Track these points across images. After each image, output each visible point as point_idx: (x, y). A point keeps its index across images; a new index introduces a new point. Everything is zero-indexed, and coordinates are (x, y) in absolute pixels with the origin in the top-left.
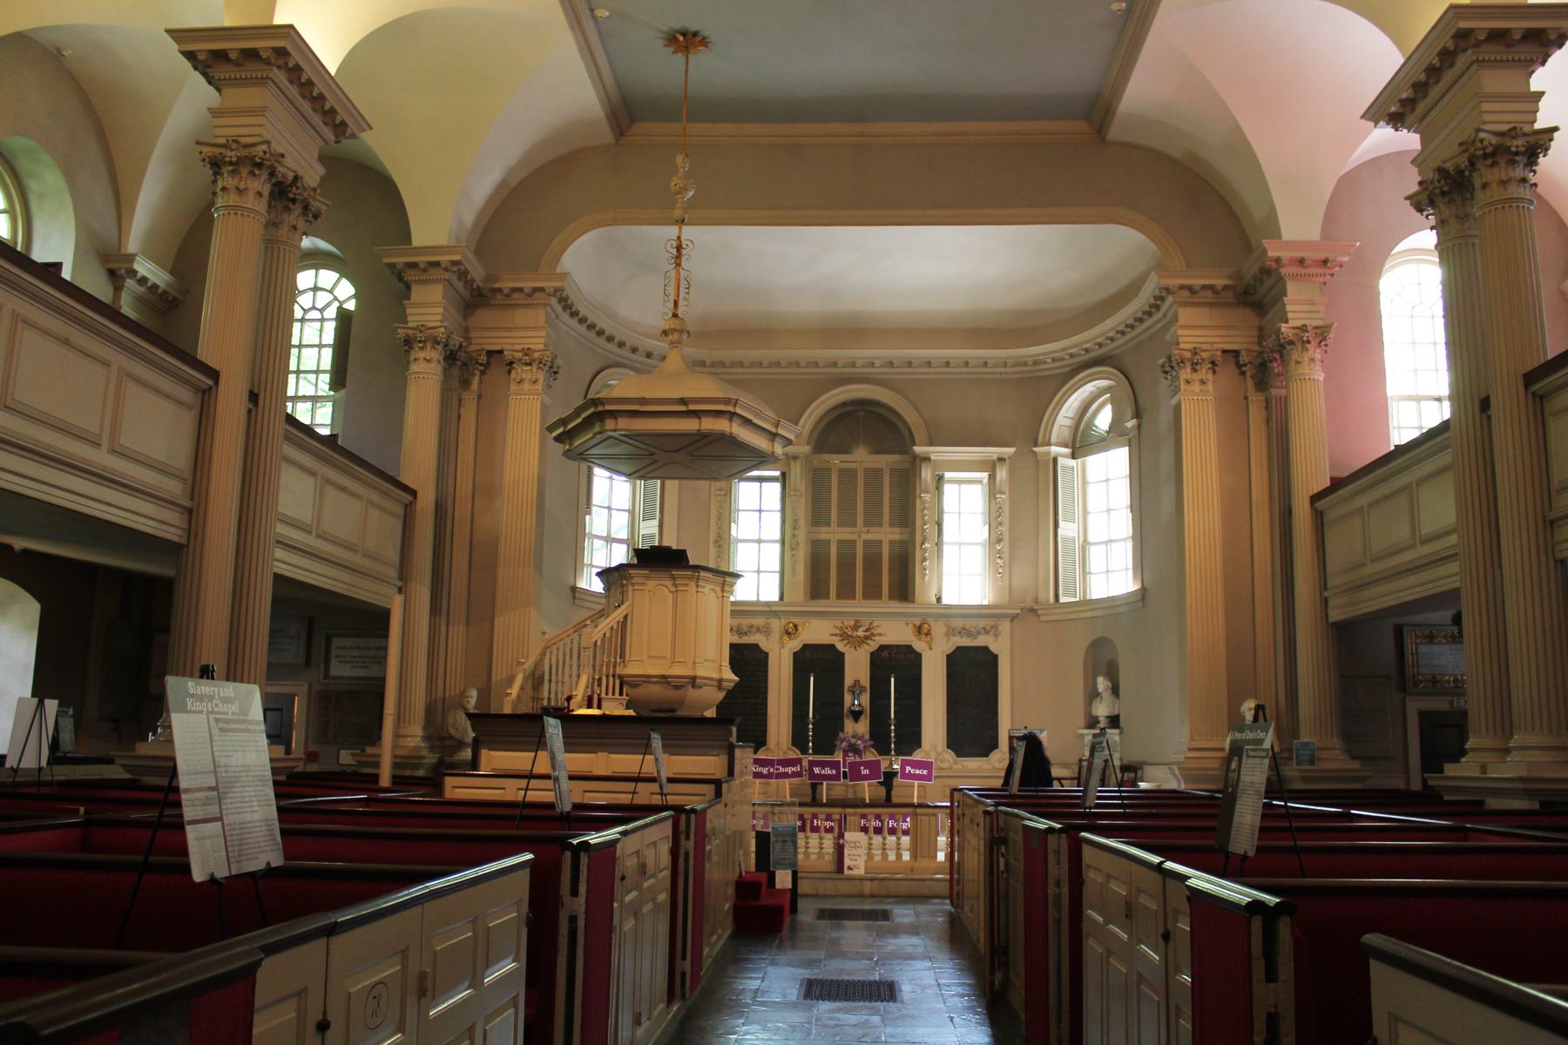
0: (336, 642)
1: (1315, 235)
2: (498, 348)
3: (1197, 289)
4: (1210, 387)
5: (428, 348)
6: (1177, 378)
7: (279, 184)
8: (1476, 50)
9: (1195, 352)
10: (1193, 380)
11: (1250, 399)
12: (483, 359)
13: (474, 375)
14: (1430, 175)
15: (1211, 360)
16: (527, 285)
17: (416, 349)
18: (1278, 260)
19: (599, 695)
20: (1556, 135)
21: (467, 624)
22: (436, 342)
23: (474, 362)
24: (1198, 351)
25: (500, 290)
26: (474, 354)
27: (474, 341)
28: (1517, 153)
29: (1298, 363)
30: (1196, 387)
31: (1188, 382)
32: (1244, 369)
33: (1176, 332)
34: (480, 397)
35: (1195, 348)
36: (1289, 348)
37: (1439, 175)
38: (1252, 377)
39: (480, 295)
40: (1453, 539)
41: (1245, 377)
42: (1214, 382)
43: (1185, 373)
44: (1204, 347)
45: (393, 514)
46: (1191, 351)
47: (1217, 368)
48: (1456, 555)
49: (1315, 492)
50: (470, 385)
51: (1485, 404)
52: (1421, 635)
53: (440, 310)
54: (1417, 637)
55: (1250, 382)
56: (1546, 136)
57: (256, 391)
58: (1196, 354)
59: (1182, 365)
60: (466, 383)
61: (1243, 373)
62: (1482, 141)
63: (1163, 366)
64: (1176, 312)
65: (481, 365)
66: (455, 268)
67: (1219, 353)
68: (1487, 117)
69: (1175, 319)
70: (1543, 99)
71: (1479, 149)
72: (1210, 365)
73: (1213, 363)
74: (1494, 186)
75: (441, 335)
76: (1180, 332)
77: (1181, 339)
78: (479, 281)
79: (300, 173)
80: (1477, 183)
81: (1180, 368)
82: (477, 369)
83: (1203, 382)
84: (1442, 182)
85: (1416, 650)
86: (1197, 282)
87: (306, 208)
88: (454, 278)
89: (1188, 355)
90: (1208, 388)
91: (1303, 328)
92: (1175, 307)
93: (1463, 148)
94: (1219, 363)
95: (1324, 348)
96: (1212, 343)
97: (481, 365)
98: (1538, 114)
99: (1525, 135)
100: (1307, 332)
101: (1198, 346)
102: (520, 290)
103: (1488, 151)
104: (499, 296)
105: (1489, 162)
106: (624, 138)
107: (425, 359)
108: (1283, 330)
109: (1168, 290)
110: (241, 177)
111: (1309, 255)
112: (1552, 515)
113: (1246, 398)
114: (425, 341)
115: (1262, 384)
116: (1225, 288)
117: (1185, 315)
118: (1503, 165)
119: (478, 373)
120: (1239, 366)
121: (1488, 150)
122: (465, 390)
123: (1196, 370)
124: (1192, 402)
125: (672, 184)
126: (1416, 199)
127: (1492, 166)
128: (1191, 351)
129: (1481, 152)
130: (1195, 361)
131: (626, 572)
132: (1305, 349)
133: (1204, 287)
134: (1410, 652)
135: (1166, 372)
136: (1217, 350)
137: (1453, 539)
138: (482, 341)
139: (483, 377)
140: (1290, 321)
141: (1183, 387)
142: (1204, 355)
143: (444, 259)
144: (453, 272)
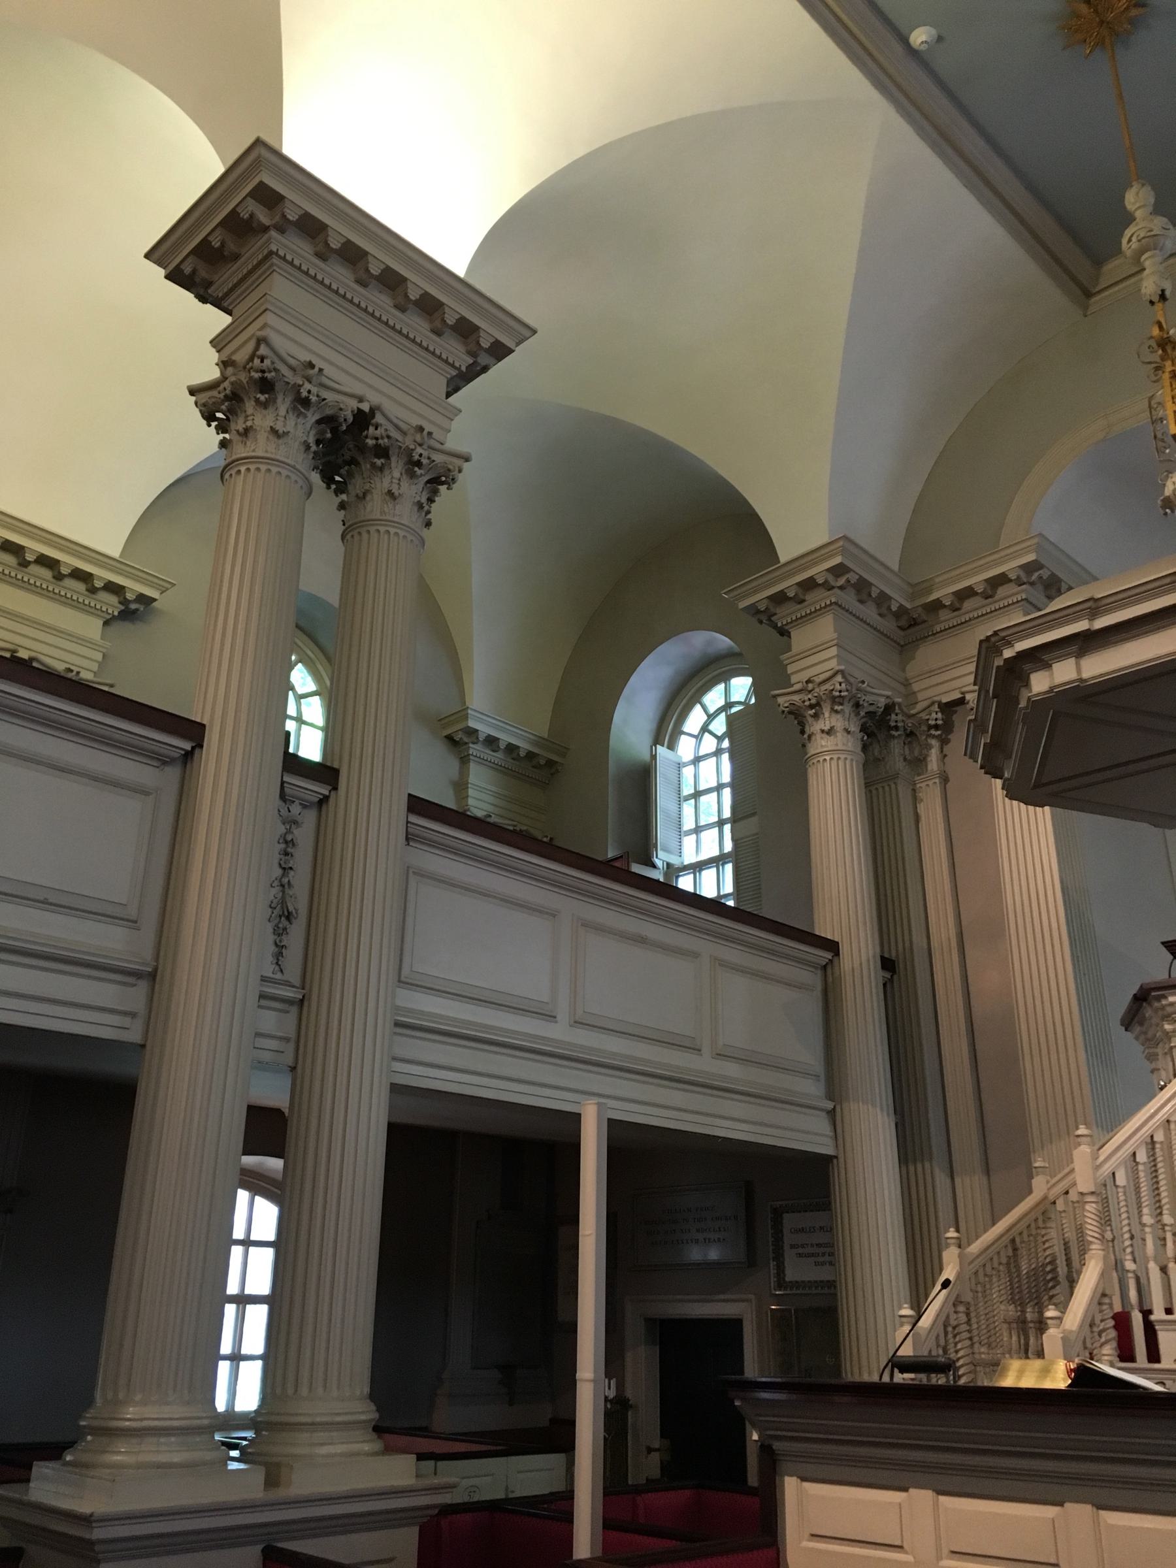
0: (789, 1220)
2: (956, 695)
5: (827, 715)
7: (329, 421)
12: (936, 717)
13: (930, 747)
16: (976, 580)
17: (810, 719)
19: (1147, 1313)
21: (988, 1172)
22: (836, 700)
23: (924, 728)
25: (937, 605)
26: (924, 716)
27: (920, 696)
34: (945, 779)
39: (914, 623)
45: (800, 987)
50: (926, 766)
53: (834, 651)
57: (336, 766)
60: (918, 763)
65: (936, 727)
66: (841, 581)
75: (838, 687)
78: (899, 599)
79: (374, 398)
82: (934, 736)
87: (413, 464)
88: (849, 599)
97: (936, 727)
102: (969, 593)
104: (944, 615)
106: (1093, 300)
107: (823, 731)
110: (247, 416)
114: (818, 704)
119: (934, 742)
122: (919, 775)
125: (1124, 240)
131: (1164, 1002)
138: (929, 693)
139: (946, 749)
143: (817, 571)
144: (841, 588)
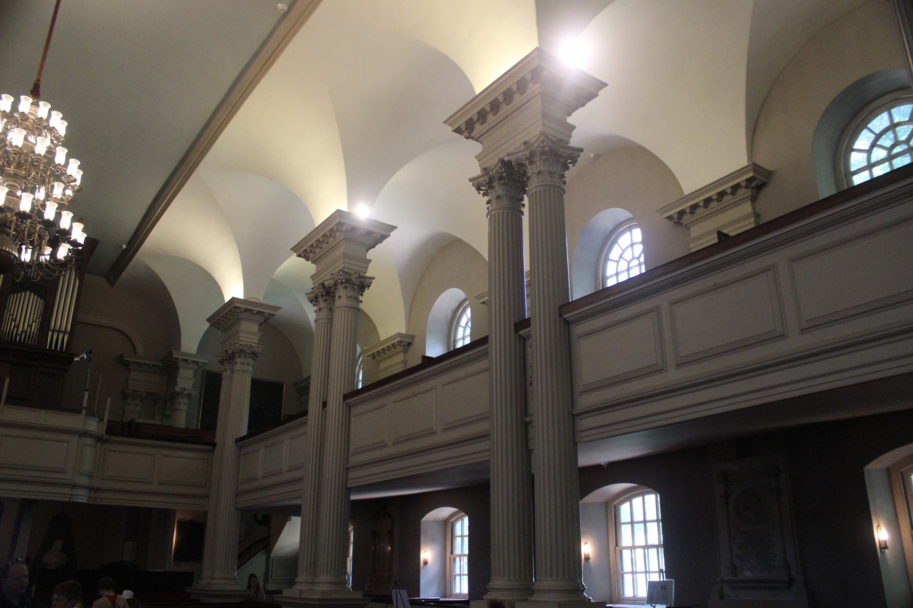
18: (177, 359)
28: (248, 353)
62: (236, 347)
68: (241, 338)
116: (154, 365)
121: (238, 351)
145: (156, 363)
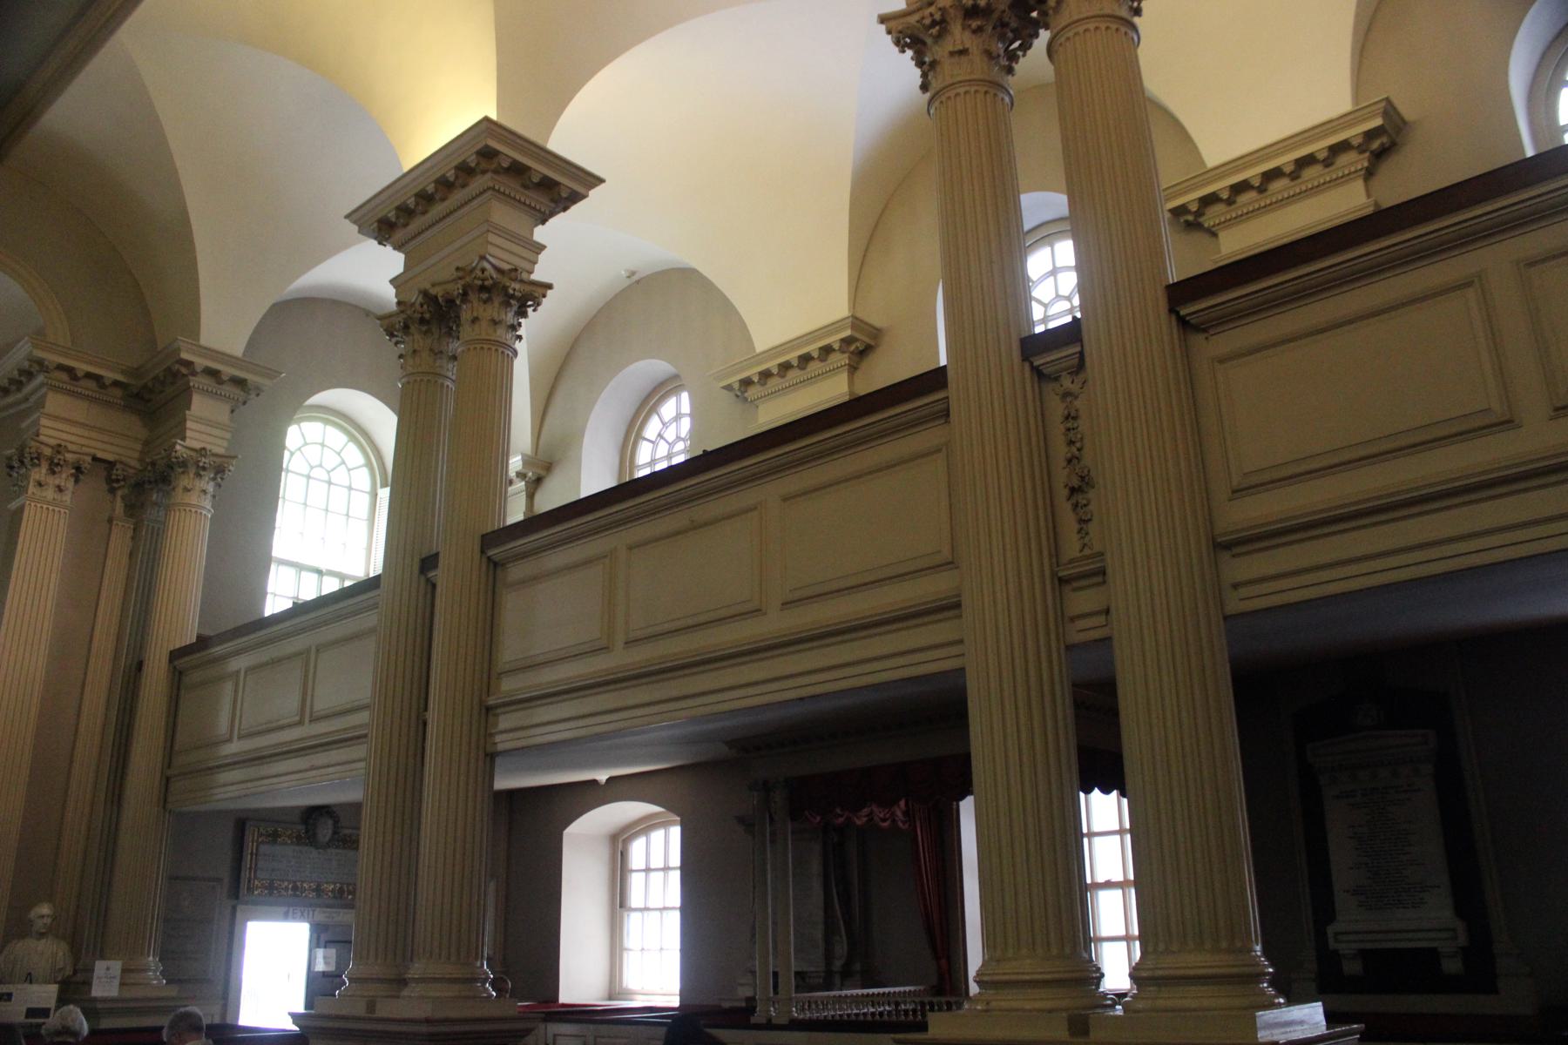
1: (237, 348)
3: (80, 374)
4: (67, 497)
6: (27, 477)
8: (495, 177)
9: (58, 449)
10: (47, 484)
11: (115, 522)
14: (414, 297)
15: (76, 465)
18: (189, 364)
20: (549, 292)
24: (61, 449)
28: (512, 297)
29: (187, 490)
30: (50, 494)
31: (40, 484)
32: (115, 485)
33: (38, 419)
35: (60, 446)
36: (180, 470)
37: (423, 298)
38: (123, 498)
40: (364, 717)
41: (115, 495)
42: (73, 493)
43: (39, 473)
44: (70, 447)
46: (52, 447)
47: (81, 477)
48: (365, 736)
49: (177, 646)
51: (429, 563)
52: (264, 832)
54: (260, 835)
55: (119, 506)
56: (540, 290)
58: (59, 452)
59: (36, 461)
61: (112, 491)
62: (483, 270)
63: (10, 458)
64: (44, 396)
67: (89, 459)
68: (492, 250)
69: (40, 404)
70: (543, 253)
71: (479, 279)
72: (73, 471)
73: (78, 469)
74: (484, 324)
76: (44, 421)
77: (43, 431)
80: (466, 315)
81: (34, 465)
83: (60, 489)
84: (425, 307)
85: (257, 850)
86: (83, 367)
89: (47, 452)
90: (64, 499)
91: (202, 452)
92: (44, 390)
93: (460, 274)
94: (86, 471)
95: (219, 480)
96: (83, 445)
98: (536, 266)
99: (522, 281)
100: (205, 457)
101: (63, 443)
103: (486, 283)
105: (485, 296)
108: (178, 447)
109: (40, 363)
111: (228, 371)
112: (491, 701)
113: (110, 521)
115: (134, 509)
116: (116, 384)
117: (56, 403)
118: (496, 304)
120: (109, 480)
123: (54, 473)
124: (39, 509)
126: (387, 321)
127: (485, 302)
128: (52, 447)
129: (480, 282)
130: (56, 461)
132: (198, 475)
133: (89, 375)
134: (250, 851)
135: (12, 468)
136: (86, 454)
137: (364, 717)
140: (188, 440)
141: (31, 489)
142: (69, 456)
145: (121, 378)
